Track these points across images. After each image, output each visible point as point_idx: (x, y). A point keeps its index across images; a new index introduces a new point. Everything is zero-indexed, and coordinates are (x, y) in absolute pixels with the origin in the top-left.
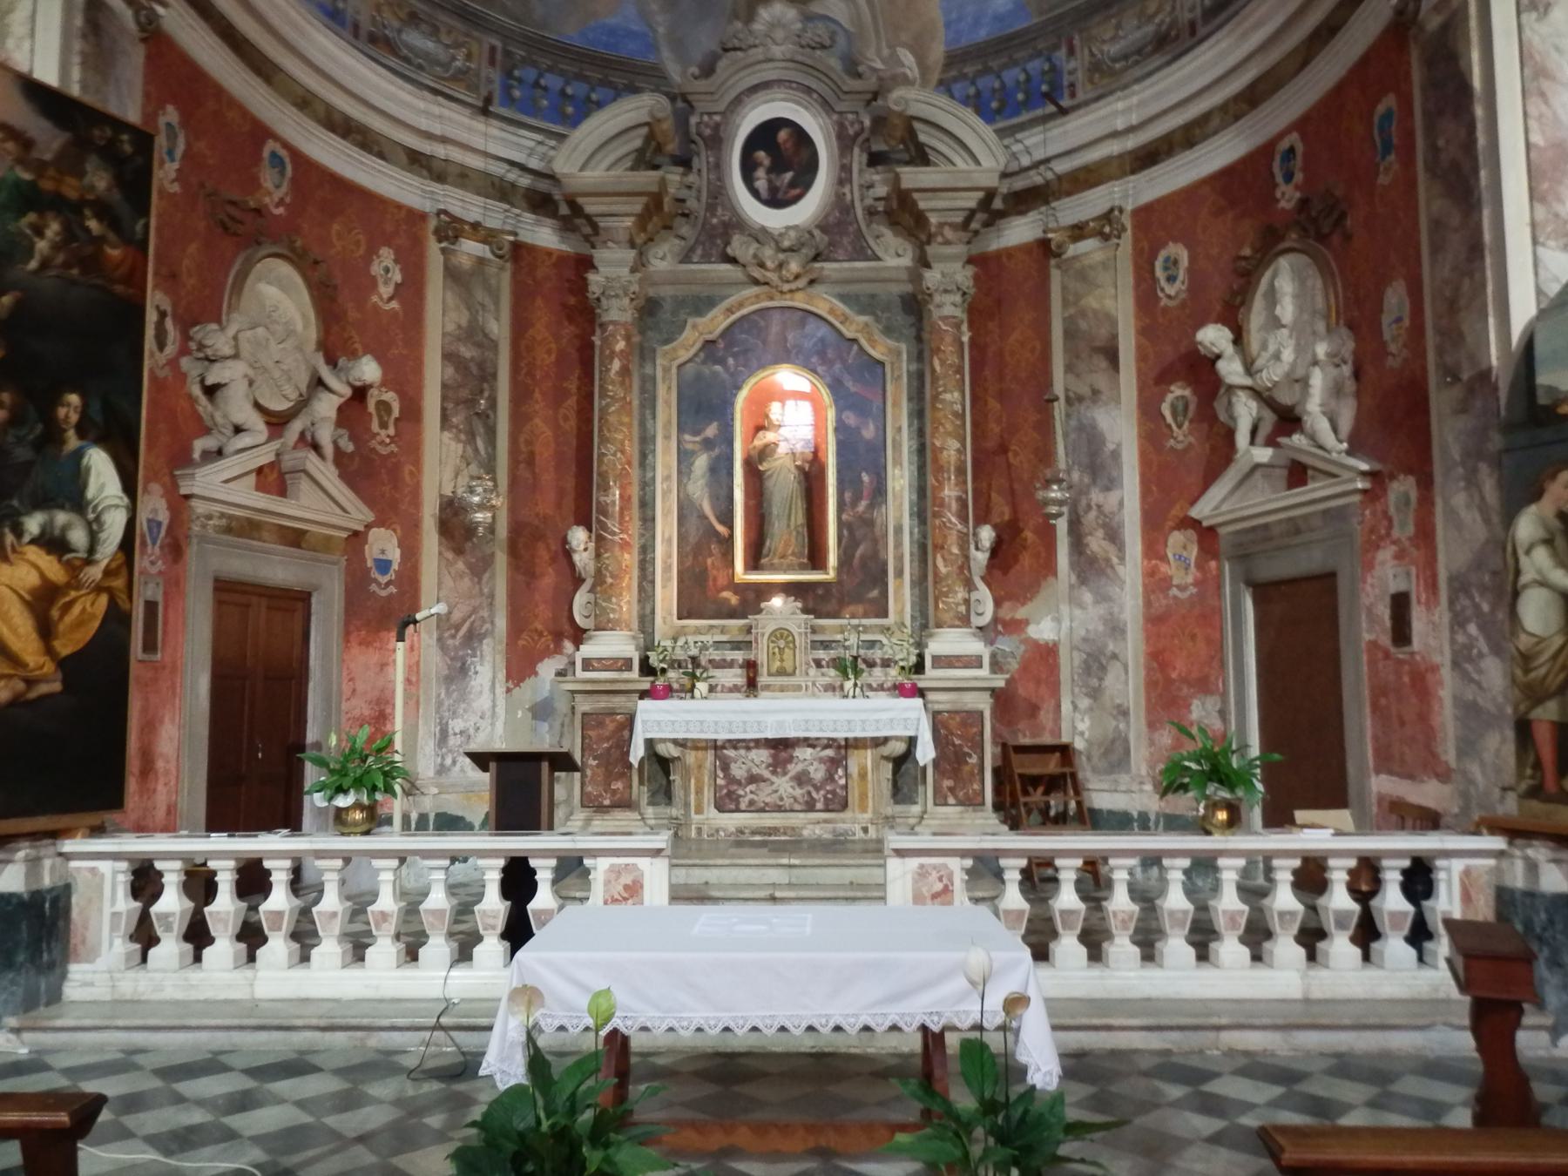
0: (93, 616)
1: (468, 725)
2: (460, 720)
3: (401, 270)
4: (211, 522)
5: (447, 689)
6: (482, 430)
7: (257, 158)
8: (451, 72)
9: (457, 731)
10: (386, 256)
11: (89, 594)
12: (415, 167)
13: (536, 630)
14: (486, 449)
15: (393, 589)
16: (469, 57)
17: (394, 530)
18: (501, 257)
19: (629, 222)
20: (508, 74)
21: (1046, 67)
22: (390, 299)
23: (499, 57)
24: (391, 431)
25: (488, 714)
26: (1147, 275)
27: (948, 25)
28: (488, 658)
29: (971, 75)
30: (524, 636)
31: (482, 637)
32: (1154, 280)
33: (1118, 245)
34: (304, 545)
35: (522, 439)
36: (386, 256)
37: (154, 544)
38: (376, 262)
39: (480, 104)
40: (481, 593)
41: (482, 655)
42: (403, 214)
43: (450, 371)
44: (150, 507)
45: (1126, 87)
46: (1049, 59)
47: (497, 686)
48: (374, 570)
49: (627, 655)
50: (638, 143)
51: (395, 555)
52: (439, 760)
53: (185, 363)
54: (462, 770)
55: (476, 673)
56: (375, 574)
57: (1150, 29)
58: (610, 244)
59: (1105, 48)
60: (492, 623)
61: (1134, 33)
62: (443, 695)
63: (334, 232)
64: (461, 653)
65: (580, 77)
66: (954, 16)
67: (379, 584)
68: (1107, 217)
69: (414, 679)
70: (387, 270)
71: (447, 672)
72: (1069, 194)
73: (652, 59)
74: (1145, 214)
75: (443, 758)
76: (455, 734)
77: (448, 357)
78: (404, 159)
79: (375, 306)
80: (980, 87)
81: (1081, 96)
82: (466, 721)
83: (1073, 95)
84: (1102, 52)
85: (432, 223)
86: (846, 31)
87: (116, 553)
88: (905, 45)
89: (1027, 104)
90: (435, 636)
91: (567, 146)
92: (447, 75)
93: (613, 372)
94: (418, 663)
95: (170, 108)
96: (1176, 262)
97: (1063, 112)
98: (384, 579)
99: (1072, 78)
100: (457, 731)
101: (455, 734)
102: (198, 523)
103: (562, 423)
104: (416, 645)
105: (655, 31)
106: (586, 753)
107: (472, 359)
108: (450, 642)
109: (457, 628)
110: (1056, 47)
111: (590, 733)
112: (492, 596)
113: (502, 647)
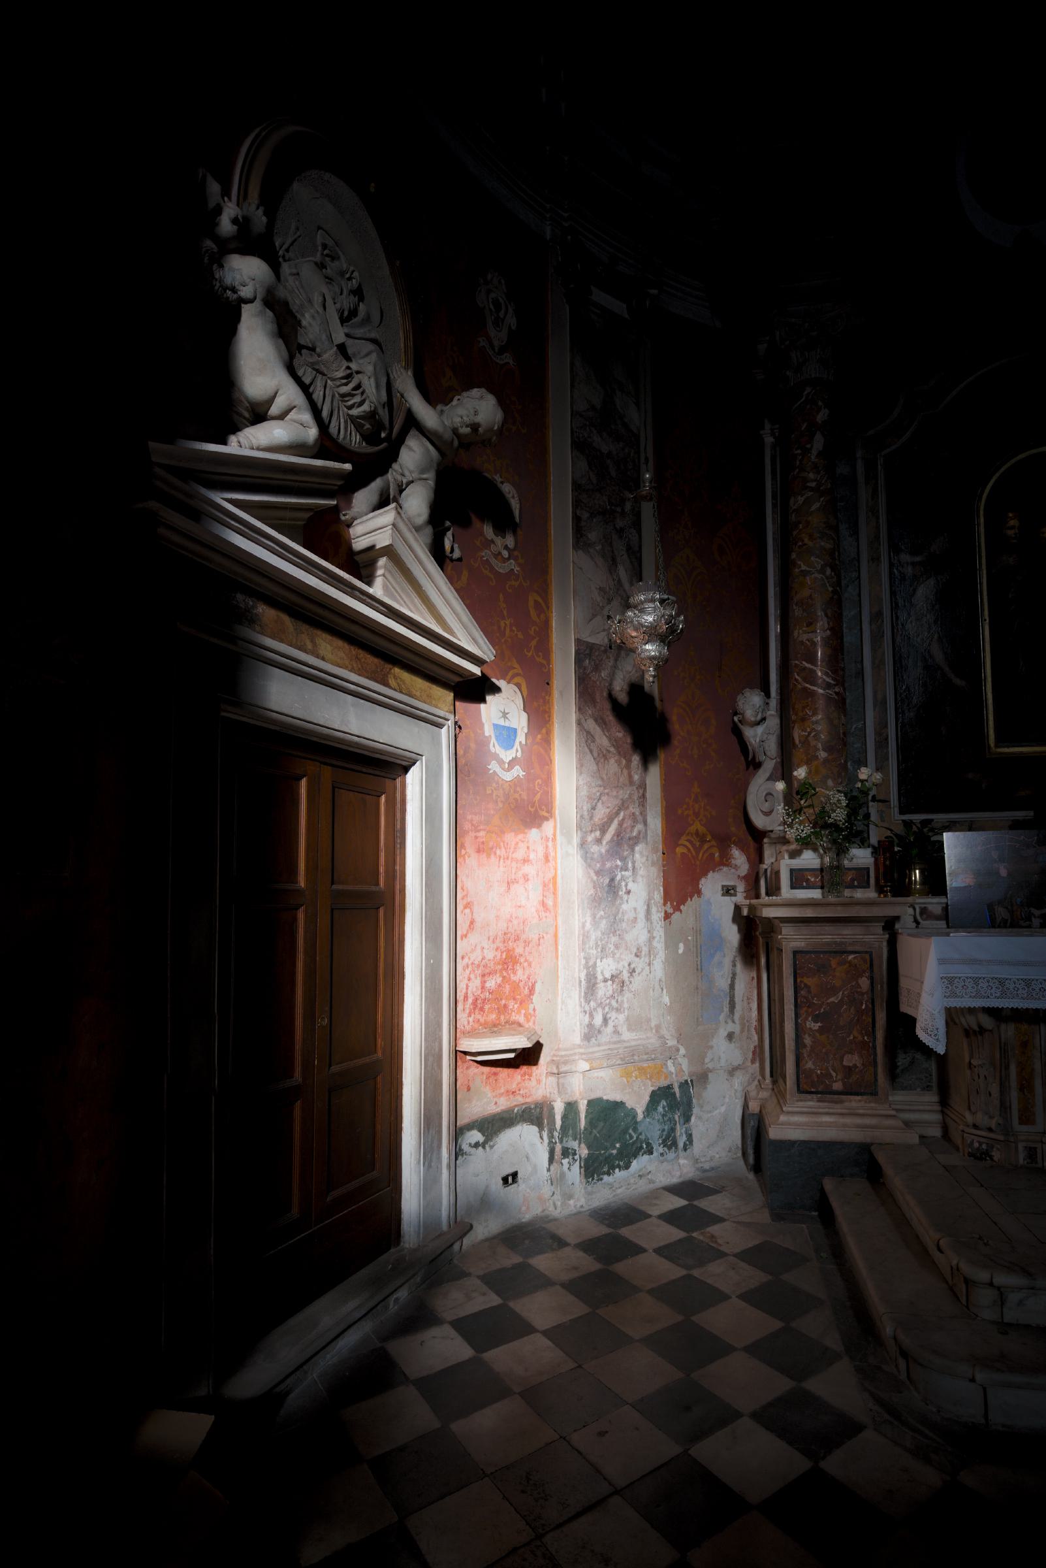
1: (620, 966)
2: (610, 960)
5: (594, 916)
9: (608, 976)
13: (697, 833)
15: (518, 771)
17: (519, 686)
25: (645, 950)
47: (654, 910)
48: (493, 740)
52: (587, 1019)
54: (616, 1032)
55: (628, 892)
56: (495, 747)
67: (501, 762)
69: (550, 903)
75: (591, 1016)
90: (576, 840)
94: (555, 878)
98: (507, 756)
101: (605, 981)
104: (552, 854)
106: (803, 1011)
111: (806, 980)
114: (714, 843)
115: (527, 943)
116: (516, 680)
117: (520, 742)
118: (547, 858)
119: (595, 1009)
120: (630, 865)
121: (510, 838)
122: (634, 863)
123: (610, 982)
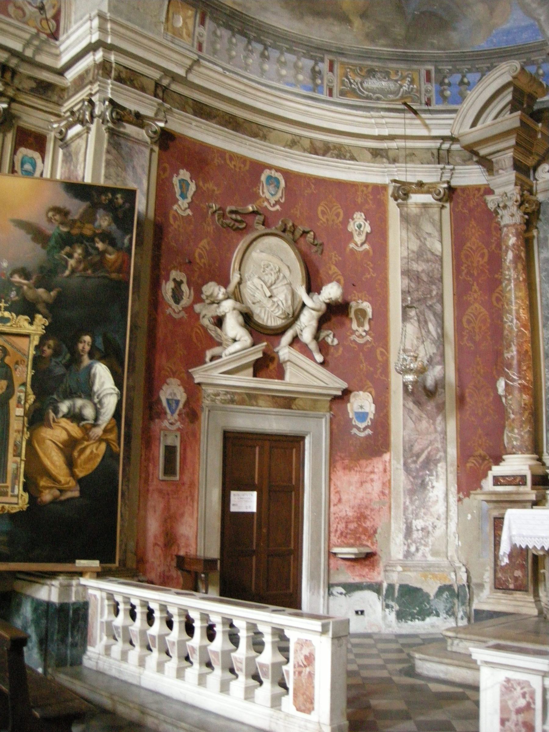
0: (97, 455)
1: (427, 524)
2: (421, 521)
3: (370, 224)
4: (218, 398)
5: (411, 499)
6: (432, 317)
7: (256, 181)
8: (400, 95)
9: (419, 528)
10: (359, 217)
11: (94, 443)
12: (378, 159)
13: (480, 456)
14: (436, 331)
15: (369, 432)
16: (412, 82)
17: (370, 393)
18: (440, 200)
19: (510, 154)
20: (442, 83)
22: (362, 244)
23: (433, 75)
24: (367, 327)
25: (443, 517)
28: (442, 476)
30: (472, 460)
31: (439, 461)
34: (294, 407)
35: (464, 320)
36: (359, 217)
37: (173, 413)
40: (436, 431)
41: (437, 475)
42: (370, 189)
43: (406, 281)
44: (169, 392)
49: (523, 473)
50: (509, 98)
51: (370, 408)
52: (406, 548)
53: (198, 308)
55: (433, 487)
56: (355, 422)
58: (501, 171)
60: (445, 452)
62: (408, 503)
64: (421, 473)
67: (358, 429)
69: (387, 492)
70: (360, 226)
71: (410, 487)
73: (540, 39)
75: (409, 547)
76: (418, 530)
77: (406, 273)
78: (369, 156)
79: (352, 250)
82: (425, 521)
85: (390, 191)
87: (111, 420)
90: (402, 462)
92: (398, 97)
93: (508, 261)
94: (390, 481)
98: (362, 425)
100: (419, 528)
102: (209, 399)
103: (495, 303)
104: (388, 468)
107: (423, 271)
108: (413, 466)
109: (418, 456)
112: (445, 433)
113: (453, 469)
114: (491, 460)
115: (372, 510)
116: (369, 390)
117: (371, 419)
118: (385, 471)
119: (411, 544)
120: (434, 473)
121: (363, 462)
122: (437, 472)
123: (420, 532)
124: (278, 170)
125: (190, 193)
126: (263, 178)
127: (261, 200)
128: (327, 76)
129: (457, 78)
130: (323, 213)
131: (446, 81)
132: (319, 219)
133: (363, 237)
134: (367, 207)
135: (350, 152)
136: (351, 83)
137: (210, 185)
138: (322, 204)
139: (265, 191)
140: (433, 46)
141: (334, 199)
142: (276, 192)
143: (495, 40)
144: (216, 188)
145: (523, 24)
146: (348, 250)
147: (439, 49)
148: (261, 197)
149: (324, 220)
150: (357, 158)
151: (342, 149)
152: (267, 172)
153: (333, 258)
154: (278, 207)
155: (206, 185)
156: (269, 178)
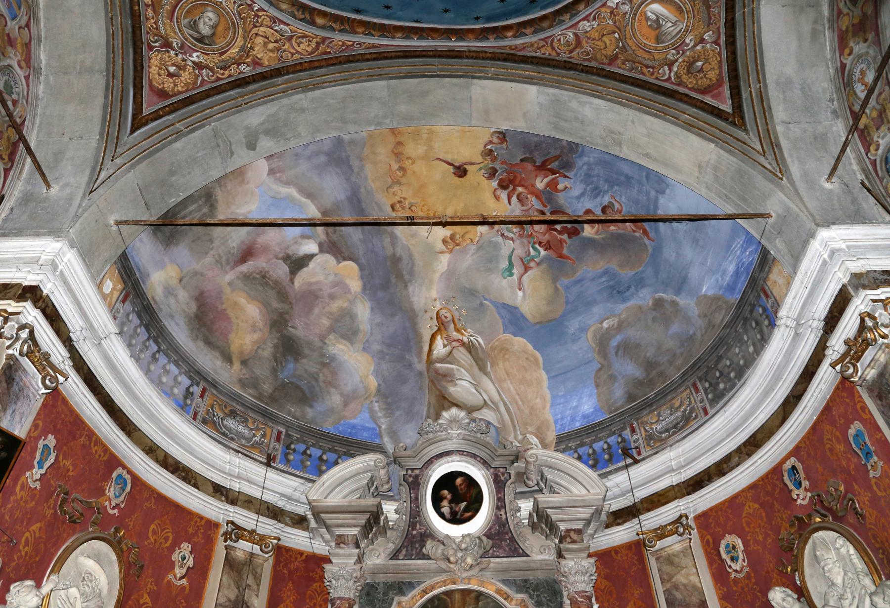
21: (620, 440)
26: (716, 558)
27: (556, 422)
29: (573, 447)
32: (723, 561)
33: (690, 539)
38: (177, 552)
39: (265, 461)
45: (671, 446)
46: (620, 436)
57: (679, 414)
59: (654, 427)
61: (668, 418)
63: (151, 530)
65: (331, 450)
66: (559, 416)
68: (678, 521)
70: (184, 558)
72: (649, 510)
74: (704, 519)
78: (211, 489)
79: (169, 582)
80: (581, 454)
81: (644, 454)
83: (639, 453)
84: (652, 429)
86: (494, 426)
88: (531, 433)
89: (610, 461)
91: (317, 485)
95: (51, 437)
96: (734, 547)
97: (636, 462)
99: (637, 444)
105: (380, 427)
110: (624, 429)
124: (130, 472)
125: (48, 464)
126: (114, 475)
127: (105, 498)
128: (197, 399)
129: (301, 447)
130: (154, 532)
131: (293, 446)
132: (148, 538)
133: (184, 571)
134: (196, 539)
135: (195, 479)
136: (214, 416)
137: (68, 463)
138: (155, 522)
139: (112, 489)
140: (289, 413)
141: (168, 521)
142: (120, 495)
143: (341, 428)
144: (71, 468)
145: (367, 425)
146: (165, 581)
147: (293, 417)
148: (106, 495)
149: (153, 540)
150: (200, 488)
151: (190, 473)
152: (119, 470)
153: (149, 586)
154: (116, 511)
155: (64, 461)
156: (120, 476)
